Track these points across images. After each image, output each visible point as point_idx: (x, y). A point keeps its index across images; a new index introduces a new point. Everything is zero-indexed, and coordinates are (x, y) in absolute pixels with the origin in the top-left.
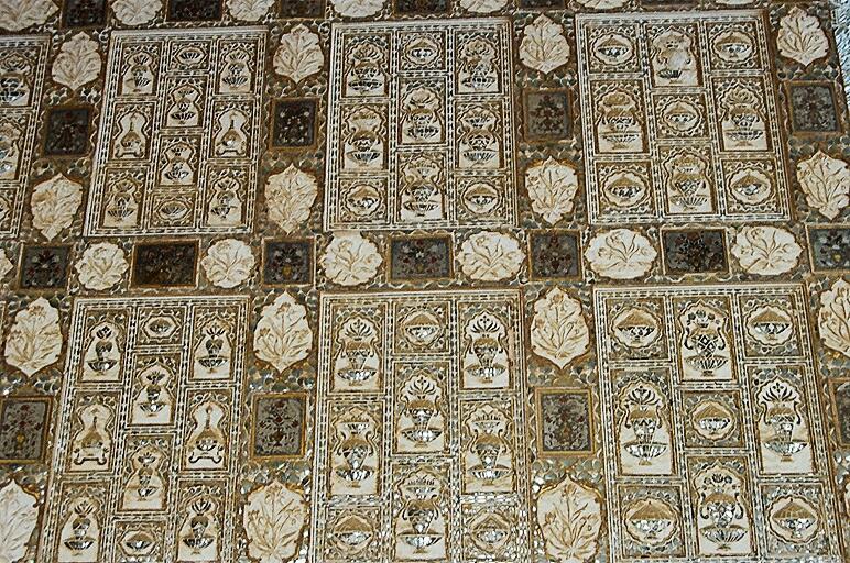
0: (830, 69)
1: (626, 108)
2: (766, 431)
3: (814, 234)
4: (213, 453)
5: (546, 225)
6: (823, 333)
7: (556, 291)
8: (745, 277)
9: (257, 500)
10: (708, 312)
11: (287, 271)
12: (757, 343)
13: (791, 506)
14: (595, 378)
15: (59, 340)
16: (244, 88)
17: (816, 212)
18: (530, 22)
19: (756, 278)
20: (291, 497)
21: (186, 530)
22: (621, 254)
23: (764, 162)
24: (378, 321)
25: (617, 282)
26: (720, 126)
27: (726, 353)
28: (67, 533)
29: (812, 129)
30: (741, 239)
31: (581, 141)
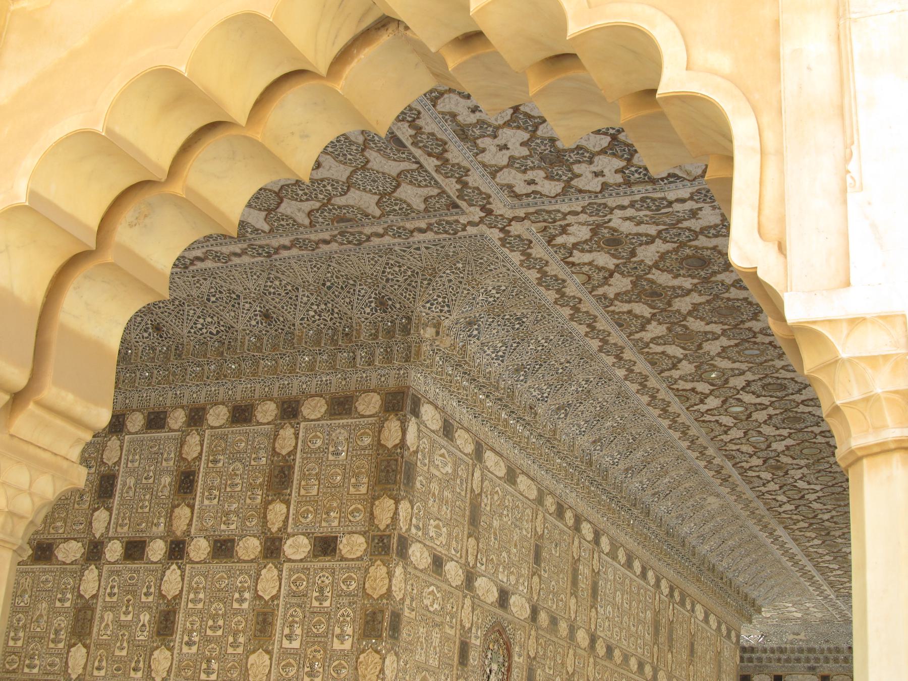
0: (399, 451)
1: (314, 472)
2: (337, 631)
4: (145, 633)
5: (272, 533)
6: (367, 586)
7: (270, 565)
8: (343, 559)
9: (156, 653)
10: (327, 575)
11: (176, 554)
12: (342, 590)
13: (340, 664)
14: (278, 605)
15: (97, 584)
16: (171, 463)
17: (377, 526)
18: (282, 428)
19: (346, 559)
20: (168, 653)
21: (133, 665)
22: (297, 547)
23: (364, 500)
24: (206, 577)
25: (294, 561)
27: (329, 594)
28: (96, 664)
29: (385, 484)
30: (344, 541)
31: (291, 491)
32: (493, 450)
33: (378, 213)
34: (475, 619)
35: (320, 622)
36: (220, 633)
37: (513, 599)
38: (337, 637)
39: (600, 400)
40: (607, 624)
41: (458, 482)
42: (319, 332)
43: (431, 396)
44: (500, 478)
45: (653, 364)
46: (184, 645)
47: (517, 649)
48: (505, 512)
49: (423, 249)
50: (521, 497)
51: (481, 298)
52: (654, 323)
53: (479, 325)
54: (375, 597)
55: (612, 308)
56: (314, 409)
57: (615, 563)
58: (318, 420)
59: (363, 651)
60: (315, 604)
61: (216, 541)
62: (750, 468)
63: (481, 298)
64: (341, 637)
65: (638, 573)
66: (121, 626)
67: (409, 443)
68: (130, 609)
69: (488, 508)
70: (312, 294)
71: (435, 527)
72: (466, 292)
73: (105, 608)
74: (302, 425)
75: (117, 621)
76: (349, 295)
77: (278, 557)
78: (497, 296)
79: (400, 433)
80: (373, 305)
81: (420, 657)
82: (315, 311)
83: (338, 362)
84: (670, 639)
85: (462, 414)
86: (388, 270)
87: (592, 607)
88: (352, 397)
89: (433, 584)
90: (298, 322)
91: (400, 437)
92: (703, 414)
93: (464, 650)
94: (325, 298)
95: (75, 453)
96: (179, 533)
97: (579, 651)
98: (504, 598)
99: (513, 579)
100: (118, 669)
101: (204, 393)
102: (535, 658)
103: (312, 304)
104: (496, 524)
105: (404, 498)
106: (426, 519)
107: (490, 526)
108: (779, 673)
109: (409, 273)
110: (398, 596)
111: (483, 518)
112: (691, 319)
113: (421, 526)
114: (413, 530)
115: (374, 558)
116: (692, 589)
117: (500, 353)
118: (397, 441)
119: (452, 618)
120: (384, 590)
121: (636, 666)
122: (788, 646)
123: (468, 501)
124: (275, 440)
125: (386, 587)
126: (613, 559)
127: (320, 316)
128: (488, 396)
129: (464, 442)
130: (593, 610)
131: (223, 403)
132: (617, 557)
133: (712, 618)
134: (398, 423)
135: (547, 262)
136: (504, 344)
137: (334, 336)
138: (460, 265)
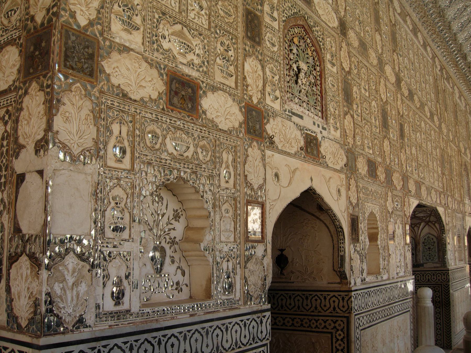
40: (406, 72)
47: (328, 57)
57: (405, 26)
87: (394, 51)
97: (389, 85)
102: (349, 72)
116: (452, 71)
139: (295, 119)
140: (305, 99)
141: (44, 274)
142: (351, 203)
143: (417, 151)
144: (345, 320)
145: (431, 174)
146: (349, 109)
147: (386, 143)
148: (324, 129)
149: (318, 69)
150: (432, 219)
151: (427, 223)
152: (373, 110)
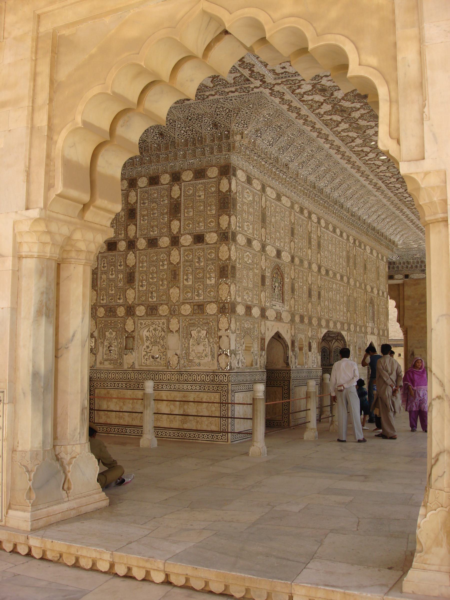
1: (190, 205)
2: (208, 276)
3: (220, 234)
5: (174, 234)
6: (219, 255)
8: (207, 244)
9: (128, 291)
12: (208, 258)
13: (211, 290)
14: (180, 266)
15: (97, 263)
17: (222, 228)
18: (173, 186)
19: (209, 244)
20: (133, 291)
21: (118, 297)
22: (186, 240)
24: (146, 256)
25: (186, 246)
26: (207, 208)
27: (203, 260)
28: (101, 298)
30: (207, 236)
32: (269, 186)
33: (212, 85)
34: (267, 265)
35: (200, 273)
36: (155, 280)
37: (283, 254)
38: (208, 278)
39: (318, 158)
41: (255, 204)
42: (186, 141)
43: (241, 166)
44: (274, 199)
45: (343, 141)
46: (140, 287)
47: (286, 276)
48: (277, 215)
49: (234, 100)
50: (283, 206)
51: (261, 119)
52: (343, 123)
53: (261, 131)
54: (224, 260)
55: (323, 118)
56: (187, 176)
57: (328, 231)
58: (190, 181)
59: (221, 284)
60: (197, 264)
61: (149, 240)
62: (390, 183)
63: (261, 119)
64: (210, 278)
65: (339, 234)
66: (110, 280)
67: (232, 189)
68: (114, 272)
69: (269, 214)
70: (182, 123)
71: (247, 226)
72: (254, 117)
73: (102, 273)
74: (183, 184)
75: (108, 278)
76: (200, 123)
77: (178, 245)
78: (269, 117)
79: (228, 185)
80: (211, 126)
81: (245, 284)
82: (184, 131)
83: (197, 154)
84: (355, 264)
85: (255, 172)
86: (217, 110)
87: (318, 253)
88: (204, 169)
89: (248, 252)
90: (176, 137)
91: (228, 187)
92: (367, 161)
93: (263, 278)
94: (188, 125)
95: (109, 224)
96: (131, 237)
97: (313, 273)
98: (279, 254)
99: (282, 244)
100: (111, 299)
101: (135, 172)
102: (294, 279)
103: (183, 128)
104: (273, 220)
105: (232, 215)
106: (242, 222)
107: (271, 222)
108: (407, 274)
109: (228, 111)
110: (233, 258)
111: (267, 219)
112: (360, 120)
113: (241, 226)
114: (238, 228)
115: (222, 243)
116: (364, 239)
117: (271, 143)
118: (227, 189)
119: (257, 265)
120: (227, 257)
121: (340, 278)
122: (411, 261)
123: (260, 212)
124: (171, 191)
125: (228, 255)
126: (327, 229)
127: (186, 133)
128: (266, 162)
129: (257, 185)
130: (319, 254)
131: (144, 176)
132: (329, 228)
133: (374, 251)
134: (227, 181)
135: (292, 101)
136: (273, 138)
137: (193, 141)
138: (251, 106)
139: (274, 307)
140: (277, 297)
141: (229, 358)
142: (292, 335)
143: (328, 303)
144: (288, 381)
145: (338, 313)
146: (293, 295)
147: (310, 304)
148: (283, 307)
149: (282, 283)
150: (339, 338)
151: (336, 340)
152: (304, 290)
